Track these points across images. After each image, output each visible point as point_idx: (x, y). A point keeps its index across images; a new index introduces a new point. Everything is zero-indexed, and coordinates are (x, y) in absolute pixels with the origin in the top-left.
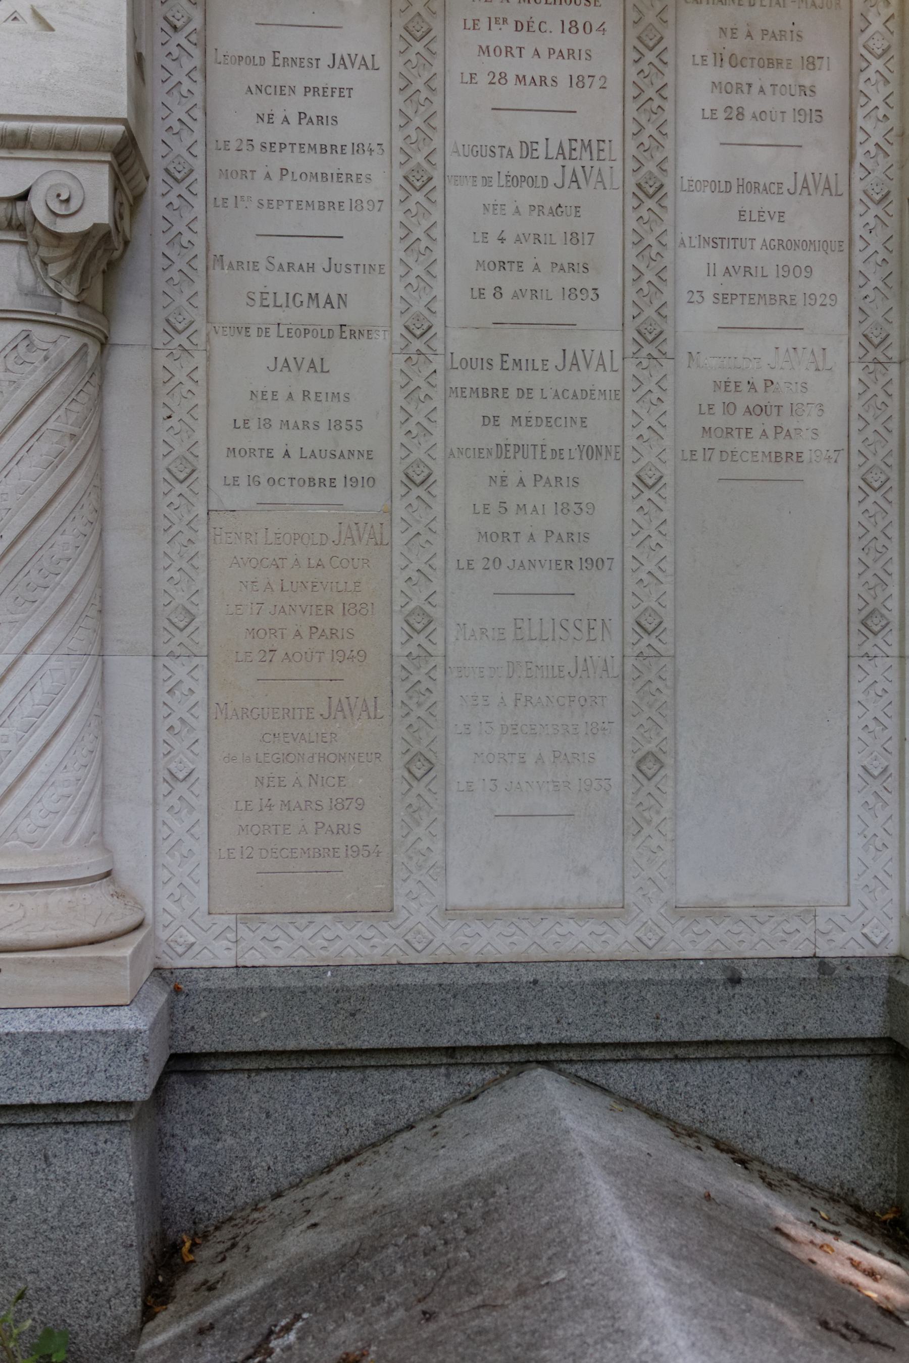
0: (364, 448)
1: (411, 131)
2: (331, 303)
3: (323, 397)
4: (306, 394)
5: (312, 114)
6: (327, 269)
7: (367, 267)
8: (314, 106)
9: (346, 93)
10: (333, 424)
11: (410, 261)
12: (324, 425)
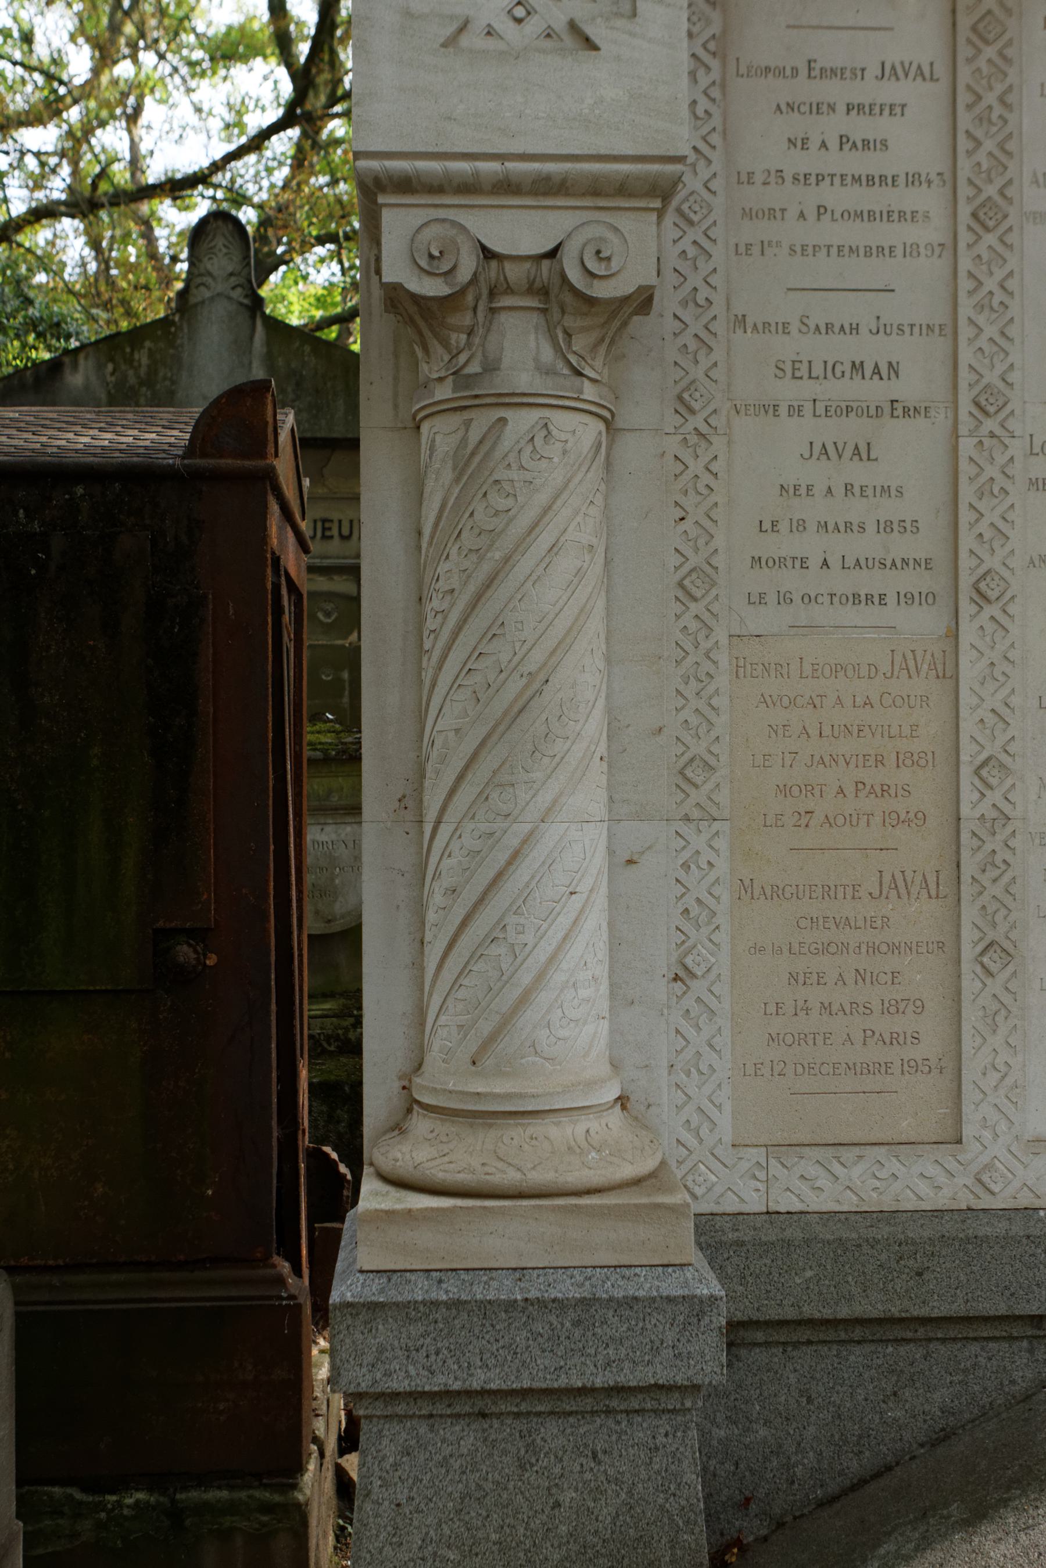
0: (921, 555)
1: (981, 156)
2: (879, 373)
3: (870, 492)
4: (848, 488)
5: (857, 137)
6: (874, 331)
7: (924, 328)
8: (861, 127)
9: (898, 110)
10: (882, 526)
11: (981, 320)
12: (871, 528)
